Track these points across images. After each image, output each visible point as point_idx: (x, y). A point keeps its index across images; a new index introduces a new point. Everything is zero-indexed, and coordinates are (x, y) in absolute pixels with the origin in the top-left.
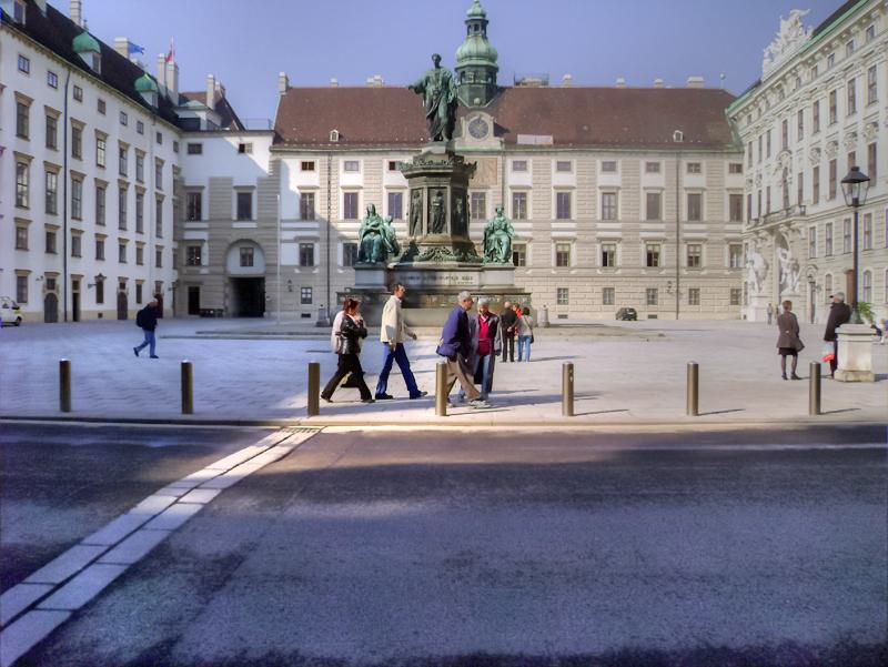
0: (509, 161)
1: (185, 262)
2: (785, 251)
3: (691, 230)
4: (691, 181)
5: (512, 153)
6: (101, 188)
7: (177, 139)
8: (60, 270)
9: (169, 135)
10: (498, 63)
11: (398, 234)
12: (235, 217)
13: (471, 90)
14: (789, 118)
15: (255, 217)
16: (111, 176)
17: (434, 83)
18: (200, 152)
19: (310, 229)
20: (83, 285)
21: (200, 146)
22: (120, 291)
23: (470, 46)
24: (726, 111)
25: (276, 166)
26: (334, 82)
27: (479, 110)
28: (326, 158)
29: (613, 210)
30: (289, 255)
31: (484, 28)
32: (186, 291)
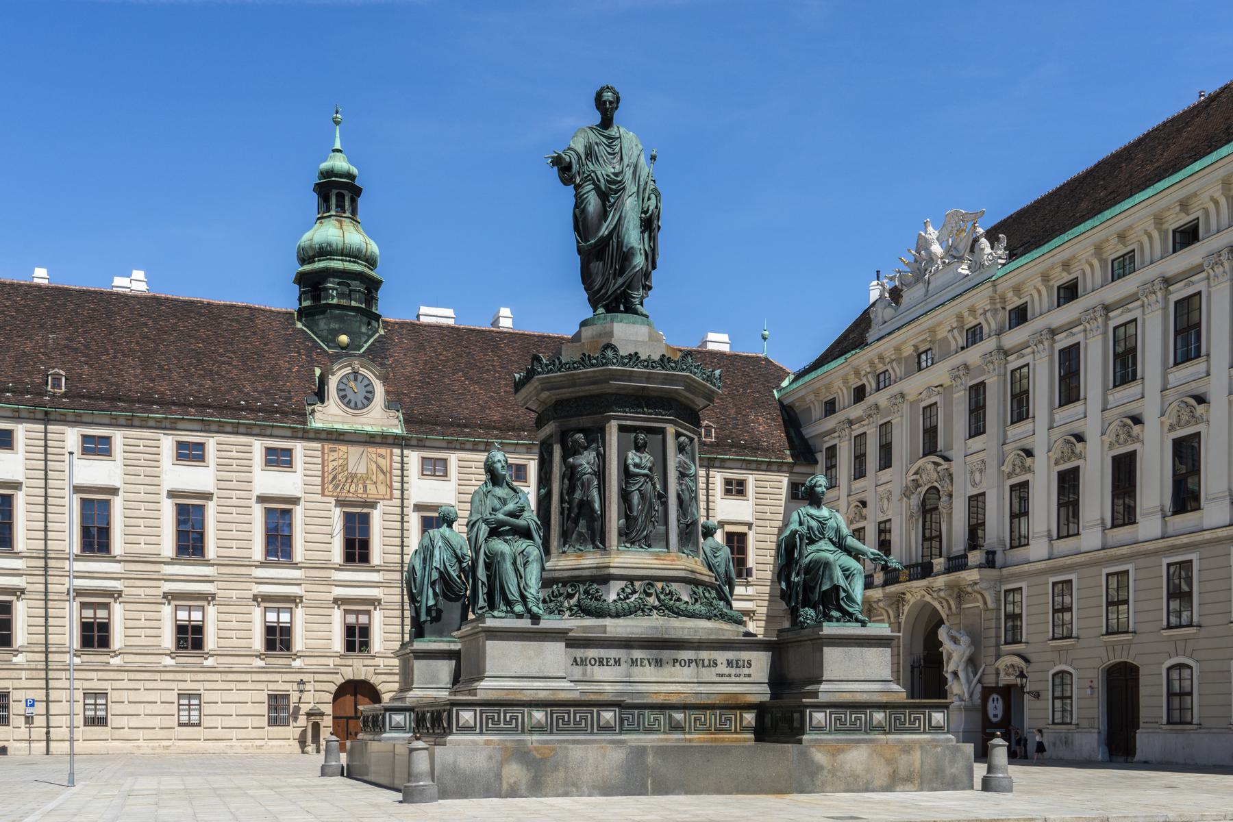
27: (348, 355)
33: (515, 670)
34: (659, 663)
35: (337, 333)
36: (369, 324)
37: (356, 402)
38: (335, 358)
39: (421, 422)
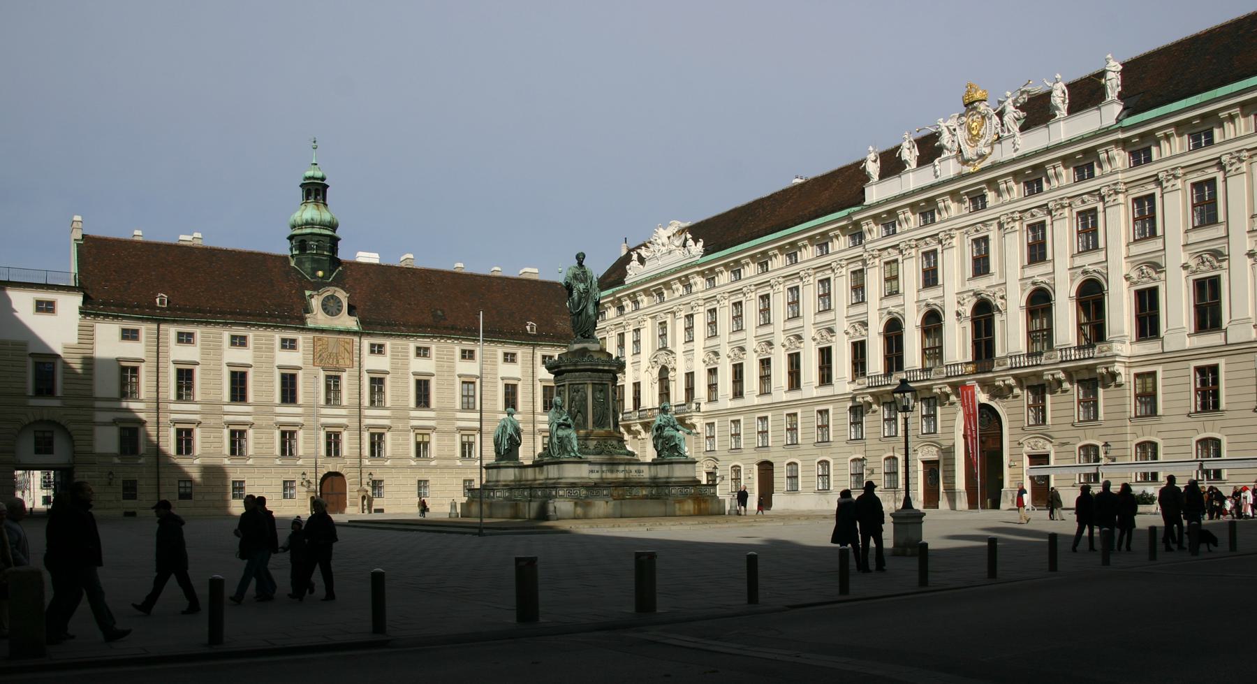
0: (366, 342)
5: (368, 334)
10: (338, 233)
14: (669, 319)
17: (582, 281)
23: (310, 212)
26: (138, 234)
28: (155, 326)
29: (471, 400)
33: (572, 475)
34: (612, 472)
35: (315, 270)
38: (317, 286)
39: (370, 323)
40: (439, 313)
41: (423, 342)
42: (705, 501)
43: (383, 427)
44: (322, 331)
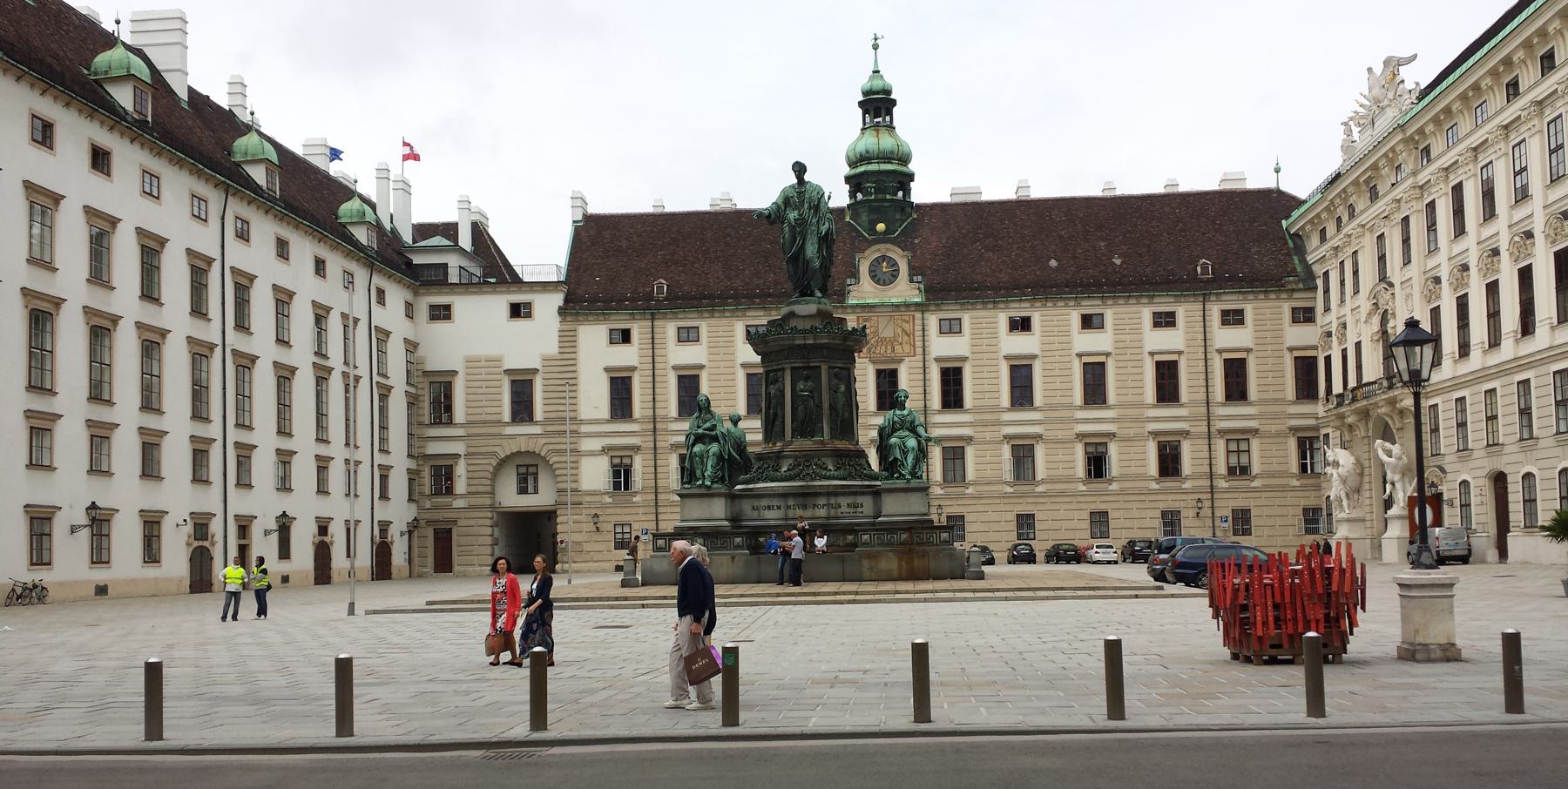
1: (427, 490)
2: (1388, 445)
3: (1232, 416)
4: (1228, 338)
5: (938, 308)
6: (284, 375)
7: (409, 296)
8: (217, 509)
9: (397, 296)
10: (912, 167)
11: (749, 437)
12: (507, 417)
13: (872, 210)
14: (1386, 231)
15: (539, 414)
16: (301, 356)
17: (797, 208)
18: (448, 317)
19: (628, 433)
20: (256, 531)
21: (448, 308)
22: (318, 539)
24: (1284, 223)
25: (568, 342)
30: (595, 474)
31: (890, 113)
32: (430, 533)
33: (696, 515)
34: (805, 507)
35: (873, 223)
36: (903, 210)
37: (883, 278)
38: (871, 243)
40: (1053, 263)
41: (1019, 311)
42: (924, 555)
43: (961, 438)
44: (871, 307)
